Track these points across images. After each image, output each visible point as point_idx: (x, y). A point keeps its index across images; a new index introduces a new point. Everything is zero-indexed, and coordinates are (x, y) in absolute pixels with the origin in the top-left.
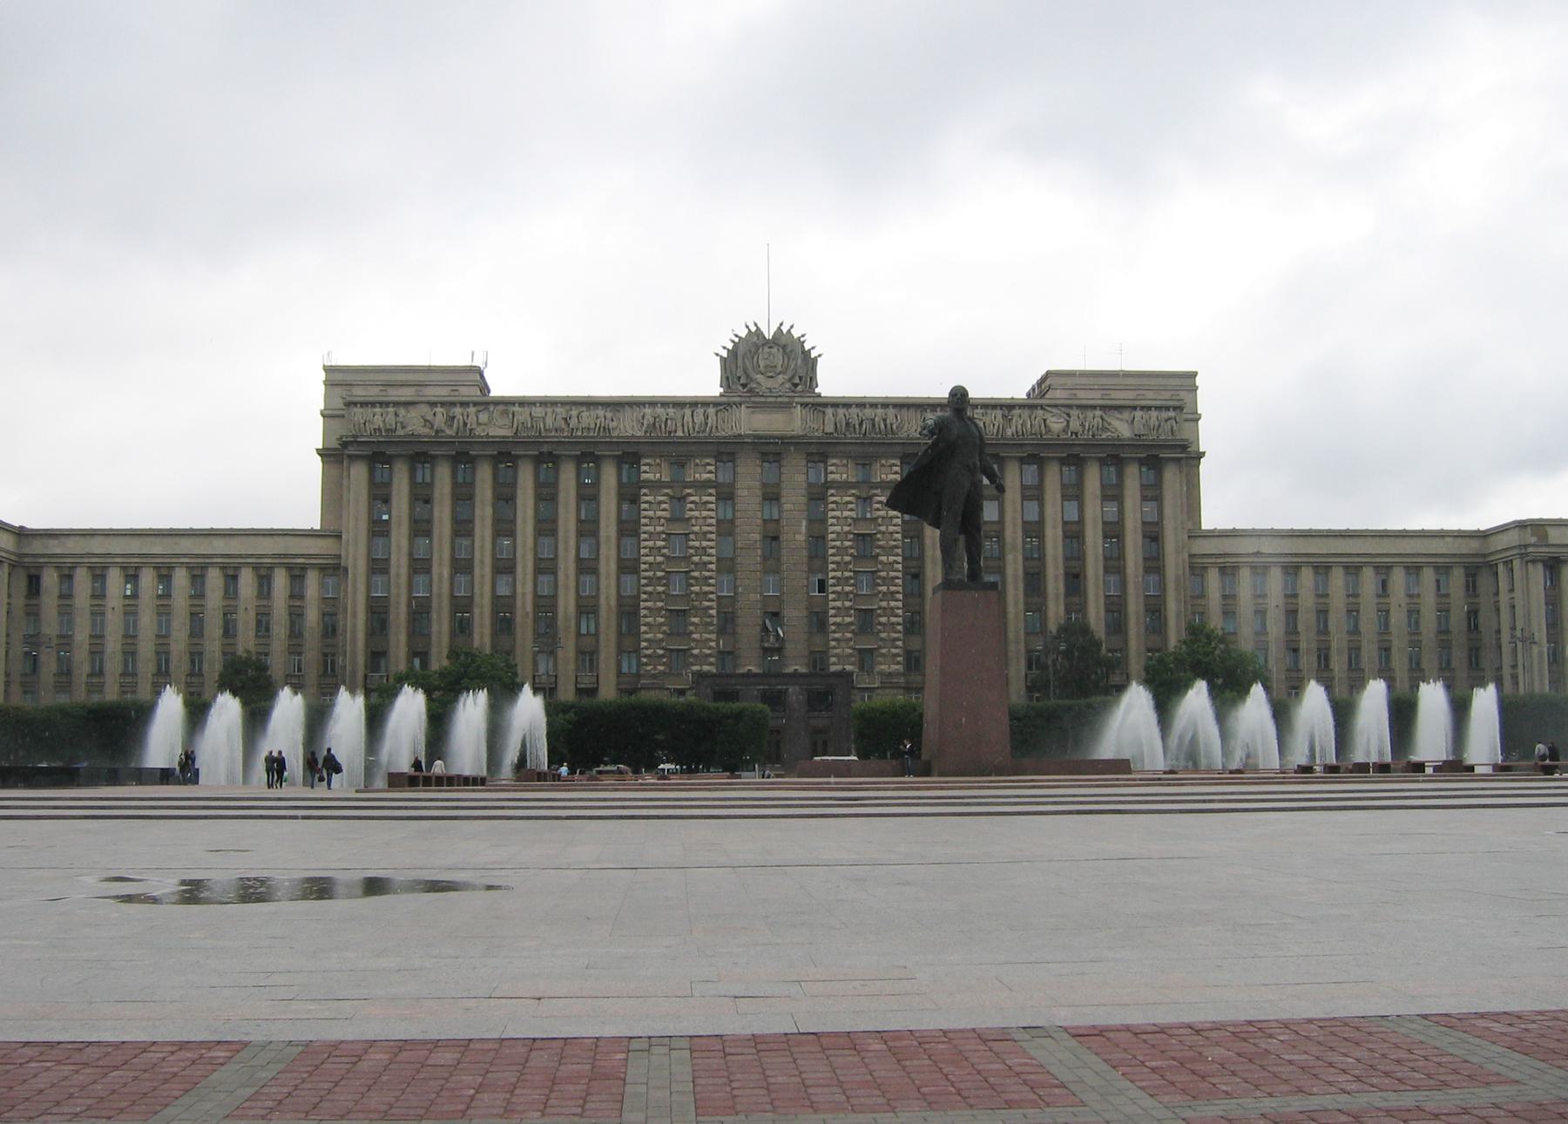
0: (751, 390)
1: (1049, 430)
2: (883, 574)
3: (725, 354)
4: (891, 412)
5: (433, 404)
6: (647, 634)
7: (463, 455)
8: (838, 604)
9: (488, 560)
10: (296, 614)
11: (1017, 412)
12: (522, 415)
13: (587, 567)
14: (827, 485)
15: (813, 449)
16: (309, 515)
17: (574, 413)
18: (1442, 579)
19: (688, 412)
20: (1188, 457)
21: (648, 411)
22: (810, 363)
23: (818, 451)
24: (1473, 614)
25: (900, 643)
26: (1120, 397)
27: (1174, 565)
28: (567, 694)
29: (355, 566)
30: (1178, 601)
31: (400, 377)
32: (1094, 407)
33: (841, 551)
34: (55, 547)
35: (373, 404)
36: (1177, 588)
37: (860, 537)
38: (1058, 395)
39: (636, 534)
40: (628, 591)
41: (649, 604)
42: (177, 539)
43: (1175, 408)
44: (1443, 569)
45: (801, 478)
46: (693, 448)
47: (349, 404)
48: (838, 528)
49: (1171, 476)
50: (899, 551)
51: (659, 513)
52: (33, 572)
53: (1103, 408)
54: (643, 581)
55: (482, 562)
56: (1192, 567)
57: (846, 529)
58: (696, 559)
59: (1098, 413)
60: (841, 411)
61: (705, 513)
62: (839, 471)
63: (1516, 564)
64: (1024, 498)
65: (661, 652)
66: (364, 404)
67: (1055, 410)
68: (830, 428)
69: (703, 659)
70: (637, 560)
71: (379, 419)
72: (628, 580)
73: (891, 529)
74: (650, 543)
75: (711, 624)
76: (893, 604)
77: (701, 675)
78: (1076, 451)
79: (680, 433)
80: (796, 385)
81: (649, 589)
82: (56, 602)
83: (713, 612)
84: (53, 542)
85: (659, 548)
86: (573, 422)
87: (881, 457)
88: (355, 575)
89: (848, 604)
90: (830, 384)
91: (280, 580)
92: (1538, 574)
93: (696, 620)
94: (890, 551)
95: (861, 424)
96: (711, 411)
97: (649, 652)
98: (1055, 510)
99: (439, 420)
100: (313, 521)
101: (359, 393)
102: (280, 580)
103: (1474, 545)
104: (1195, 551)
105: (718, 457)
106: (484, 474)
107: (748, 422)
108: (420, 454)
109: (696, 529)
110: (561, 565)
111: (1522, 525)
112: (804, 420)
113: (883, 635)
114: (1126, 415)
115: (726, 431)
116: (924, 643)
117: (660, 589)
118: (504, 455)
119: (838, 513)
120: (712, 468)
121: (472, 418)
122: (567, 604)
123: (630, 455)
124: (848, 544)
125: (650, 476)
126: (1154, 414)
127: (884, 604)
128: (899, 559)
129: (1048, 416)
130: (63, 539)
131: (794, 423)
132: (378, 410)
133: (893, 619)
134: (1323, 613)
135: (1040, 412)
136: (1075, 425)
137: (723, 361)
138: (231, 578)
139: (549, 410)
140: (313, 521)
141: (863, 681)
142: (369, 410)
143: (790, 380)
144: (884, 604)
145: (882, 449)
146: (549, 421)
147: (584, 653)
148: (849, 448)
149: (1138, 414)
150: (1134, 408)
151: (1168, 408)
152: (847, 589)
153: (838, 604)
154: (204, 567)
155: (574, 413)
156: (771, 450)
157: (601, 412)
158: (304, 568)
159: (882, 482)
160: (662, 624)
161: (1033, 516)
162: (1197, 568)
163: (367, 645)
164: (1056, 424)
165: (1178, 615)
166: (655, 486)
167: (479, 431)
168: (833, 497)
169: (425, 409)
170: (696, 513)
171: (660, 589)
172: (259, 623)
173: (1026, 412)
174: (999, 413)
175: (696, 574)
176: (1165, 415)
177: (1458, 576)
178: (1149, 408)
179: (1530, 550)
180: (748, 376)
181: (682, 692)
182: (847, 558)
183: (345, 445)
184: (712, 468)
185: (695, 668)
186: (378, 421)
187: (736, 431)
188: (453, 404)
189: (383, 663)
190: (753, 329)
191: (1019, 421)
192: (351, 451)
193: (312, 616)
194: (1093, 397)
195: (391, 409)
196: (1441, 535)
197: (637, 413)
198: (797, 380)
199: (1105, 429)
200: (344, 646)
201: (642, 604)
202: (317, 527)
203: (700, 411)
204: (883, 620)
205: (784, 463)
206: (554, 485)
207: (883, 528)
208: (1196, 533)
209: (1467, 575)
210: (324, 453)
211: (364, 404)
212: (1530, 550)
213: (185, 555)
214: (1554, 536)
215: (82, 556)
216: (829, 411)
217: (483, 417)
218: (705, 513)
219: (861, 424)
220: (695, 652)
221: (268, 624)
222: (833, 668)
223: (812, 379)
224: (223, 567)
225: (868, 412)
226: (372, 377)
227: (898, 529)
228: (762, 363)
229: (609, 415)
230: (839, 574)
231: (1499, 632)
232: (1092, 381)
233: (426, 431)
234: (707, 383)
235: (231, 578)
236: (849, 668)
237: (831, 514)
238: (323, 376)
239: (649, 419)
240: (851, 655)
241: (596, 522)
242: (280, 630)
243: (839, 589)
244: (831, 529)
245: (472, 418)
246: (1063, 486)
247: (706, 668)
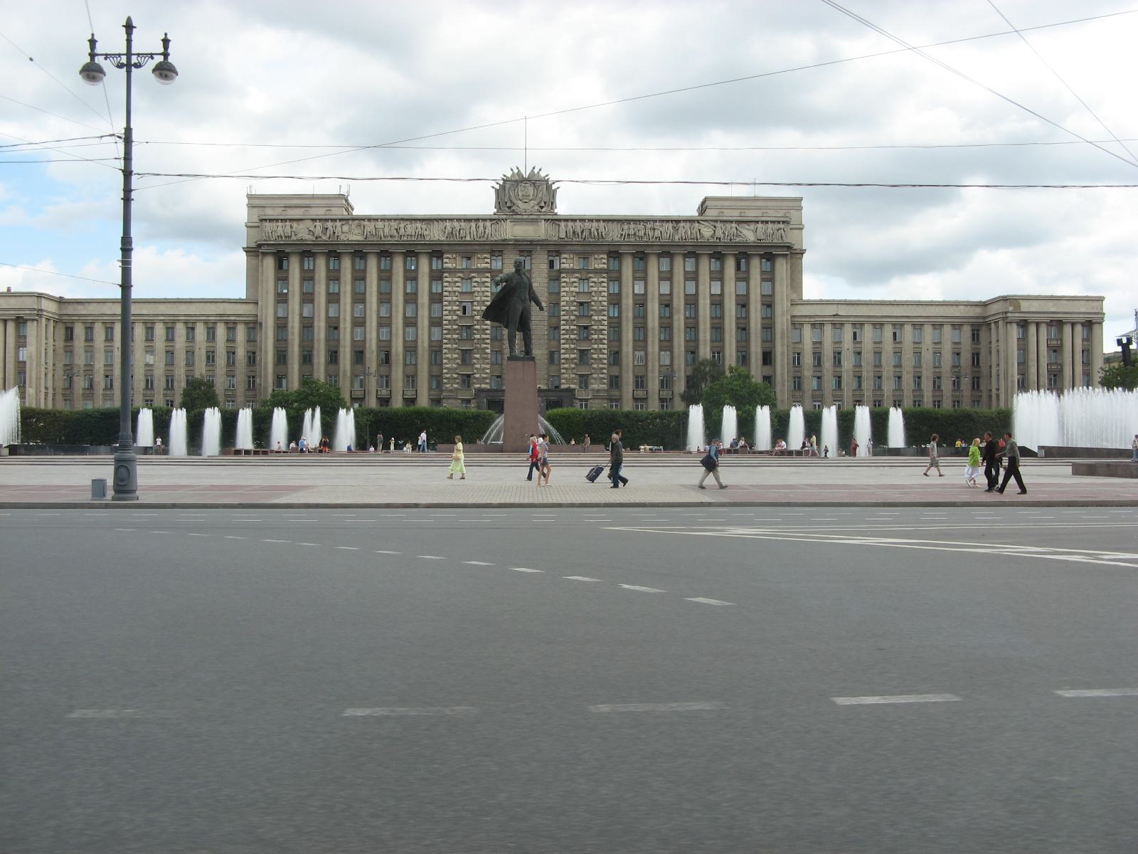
0: (513, 211)
1: (702, 236)
2: (595, 327)
3: (497, 187)
4: (602, 224)
5: (314, 220)
6: (447, 365)
7: (333, 253)
8: (567, 346)
9: (348, 318)
10: (231, 353)
11: (682, 224)
12: (370, 227)
13: (410, 322)
14: (443, 271)
15: (552, 248)
16: (239, 290)
17: (402, 226)
18: (858, 331)
19: (473, 224)
20: (794, 254)
21: (448, 224)
22: (552, 194)
23: (555, 249)
24: (976, 357)
25: (605, 371)
26: (751, 214)
27: (782, 322)
28: (372, 403)
29: (266, 322)
30: (783, 345)
31: (295, 202)
32: (732, 222)
33: (569, 313)
34: (82, 310)
35: (277, 220)
36: (782, 338)
37: (581, 304)
38: (711, 213)
39: (441, 302)
40: (436, 337)
41: (448, 346)
42: (157, 305)
43: (784, 222)
44: (957, 326)
45: (545, 267)
46: (477, 247)
47: (262, 220)
48: (567, 299)
49: (782, 267)
50: (606, 313)
51: (455, 289)
52: (68, 325)
53: (737, 222)
54: (445, 332)
55: (345, 320)
56: (793, 324)
57: (572, 299)
59: (734, 225)
60: (570, 224)
61: (483, 289)
62: (567, 262)
63: (1000, 323)
64: (686, 279)
65: (455, 376)
66: (271, 220)
67: (705, 223)
68: (563, 235)
69: (482, 380)
70: (441, 318)
71: (280, 229)
72: (436, 330)
73: (601, 299)
74: (449, 308)
75: (486, 358)
76: (601, 346)
77: (480, 391)
78: (719, 249)
79: (468, 238)
80: (542, 207)
81: (449, 336)
82: (83, 344)
83: (488, 351)
85: (455, 311)
86: (402, 231)
87: (595, 253)
88: (266, 327)
89: (572, 346)
90: (563, 208)
91: (221, 331)
92: (1014, 332)
93: (478, 356)
94: (599, 312)
95: (582, 232)
96: (488, 224)
97: (448, 376)
98: (707, 288)
99: (318, 231)
100: (242, 294)
101: (270, 213)
102: (221, 331)
103: (978, 311)
104: (796, 313)
105: (492, 253)
106: (346, 263)
107: (511, 231)
108: (307, 252)
109: (478, 299)
110: (394, 321)
111: (1005, 299)
112: (546, 230)
113: (595, 366)
114: (752, 226)
115: (497, 237)
116: (621, 371)
117: (455, 336)
118: (359, 253)
119: (567, 289)
120: (488, 260)
121: (339, 229)
122: (398, 347)
123: (437, 252)
124: (573, 308)
125: (450, 265)
126: (770, 225)
127: (595, 346)
128: (605, 318)
129: (701, 227)
130: (87, 305)
131: (540, 231)
132: (280, 224)
133: (601, 356)
134: (878, 354)
135: (696, 225)
136: (719, 233)
137: (497, 191)
138: (191, 330)
139: (387, 224)
140: (242, 294)
141: (581, 394)
142: (275, 224)
143: (538, 204)
144: (595, 346)
145: (595, 249)
146: (386, 230)
147: (408, 377)
148: (574, 248)
149: (760, 225)
150: (757, 222)
151: (779, 222)
152: (572, 336)
153: (567, 346)
154: (174, 322)
155: (402, 226)
156: (526, 248)
157: (419, 225)
158: (235, 323)
159: (595, 269)
160: (456, 358)
161: (691, 290)
162: (796, 324)
163: (274, 372)
164: (707, 232)
165: (783, 354)
166: (453, 272)
167: (343, 237)
168: (565, 279)
169: (309, 224)
170: (478, 289)
171: (455, 336)
172: (208, 358)
173: (688, 225)
174: (670, 225)
175: (478, 327)
176: (777, 226)
177: (967, 331)
178: (767, 222)
179: (1009, 315)
180: (511, 201)
181: (468, 401)
182: (573, 318)
183: (260, 246)
184: (488, 260)
185: (477, 386)
186: (280, 231)
187: (503, 237)
188: (327, 220)
189: (284, 382)
190: (516, 171)
191: (684, 230)
192: (263, 250)
193: (241, 353)
194: (734, 214)
195: (288, 223)
196: (956, 304)
197: (441, 225)
198: (543, 204)
199: (738, 236)
200: (260, 371)
201: (444, 346)
202: (244, 296)
203: (481, 224)
204: (595, 356)
205: (534, 256)
206: (390, 271)
207: (595, 299)
208: (798, 302)
209: (973, 330)
210: (248, 251)
211: (271, 220)
212: (1009, 315)
213: (162, 315)
214: (1025, 306)
215: (99, 315)
216: (563, 224)
217: (346, 228)
218: (483, 289)
219: (582, 232)
220: (477, 376)
221: (213, 357)
222: (563, 387)
223: (552, 204)
224: (186, 323)
225: (587, 224)
226: (278, 202)
227: (605, 299)
228: (520, 194)
229: (424, 227)
230: (567, 327)
231: (991, 367)
232: (733, 203)
234: (485, 204)
235: (191, 330)
236: (573, 386)
237: (562, 289)
238: (246, 201)
239: (449, 229)
240: (573, 378)
241: (416, 294)
242: (221, 360)
243: (567, 336)
244: (563, 299)
245: (339, 229)
246: (711, 272)
247: (484, 386)
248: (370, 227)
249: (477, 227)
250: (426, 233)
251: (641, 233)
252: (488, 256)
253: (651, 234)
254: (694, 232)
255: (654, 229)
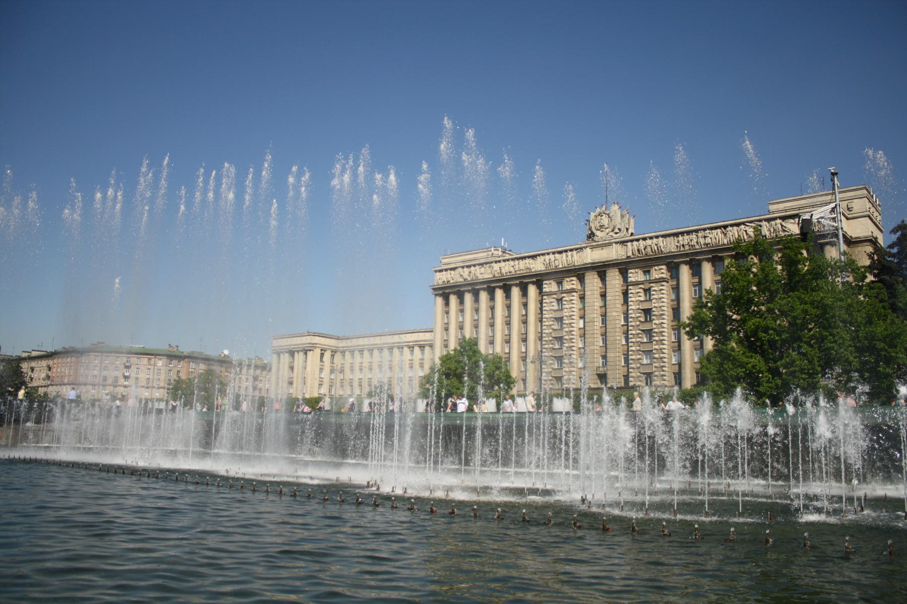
17: (517, 262)
19: (564, 254)
21: (547, 257)
53: (780, 218)
58: (567, 330)
59: (779, 221)
60: (635, 243)
84: (348, 341)
112: (617, 251)
127: (657, 347)
129: (747, 228)
135: (742, 227)
143: (613, 231)
157: (527, 261)
167: (480, 277)
169: (460, 269)
173: (735, 228)
216: (629, 244)
217: (483, 270)
225: (649, 242)
233: (462, 280)
236: (638, 383)
248: (496, 266)
249: (567, 256)
250: (532, 266)
251: (694, 242)
252: (574, 278)
253: (702, 241)
254: (740, 233)
255: (705, 237)
